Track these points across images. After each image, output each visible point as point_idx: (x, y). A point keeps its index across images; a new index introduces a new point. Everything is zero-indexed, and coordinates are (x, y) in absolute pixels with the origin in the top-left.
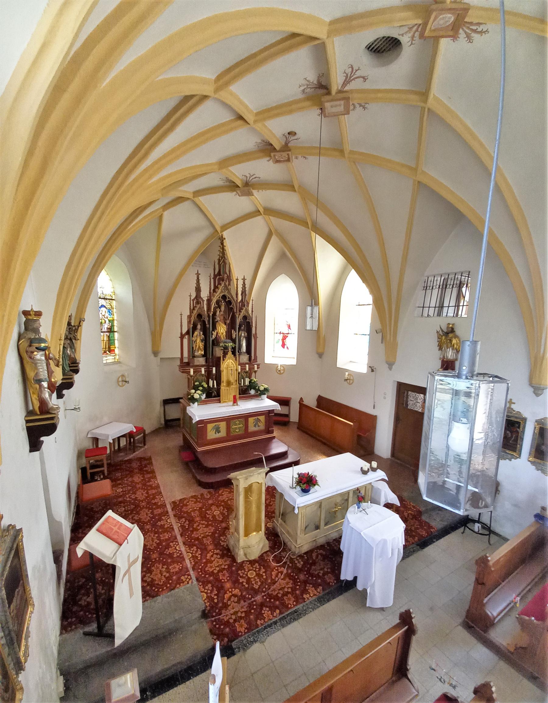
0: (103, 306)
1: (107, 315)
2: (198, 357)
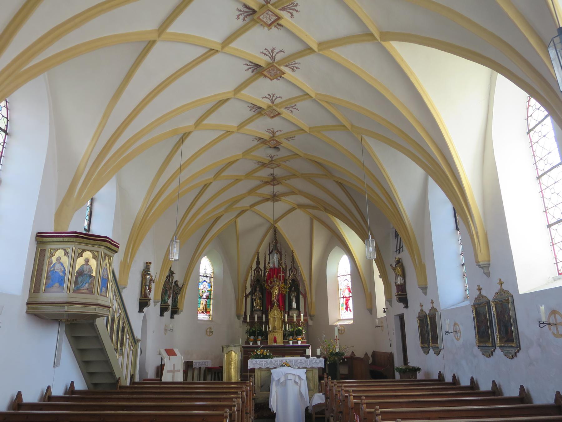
0: (204, 281)
1: (207, 287)
2: (257, 311)
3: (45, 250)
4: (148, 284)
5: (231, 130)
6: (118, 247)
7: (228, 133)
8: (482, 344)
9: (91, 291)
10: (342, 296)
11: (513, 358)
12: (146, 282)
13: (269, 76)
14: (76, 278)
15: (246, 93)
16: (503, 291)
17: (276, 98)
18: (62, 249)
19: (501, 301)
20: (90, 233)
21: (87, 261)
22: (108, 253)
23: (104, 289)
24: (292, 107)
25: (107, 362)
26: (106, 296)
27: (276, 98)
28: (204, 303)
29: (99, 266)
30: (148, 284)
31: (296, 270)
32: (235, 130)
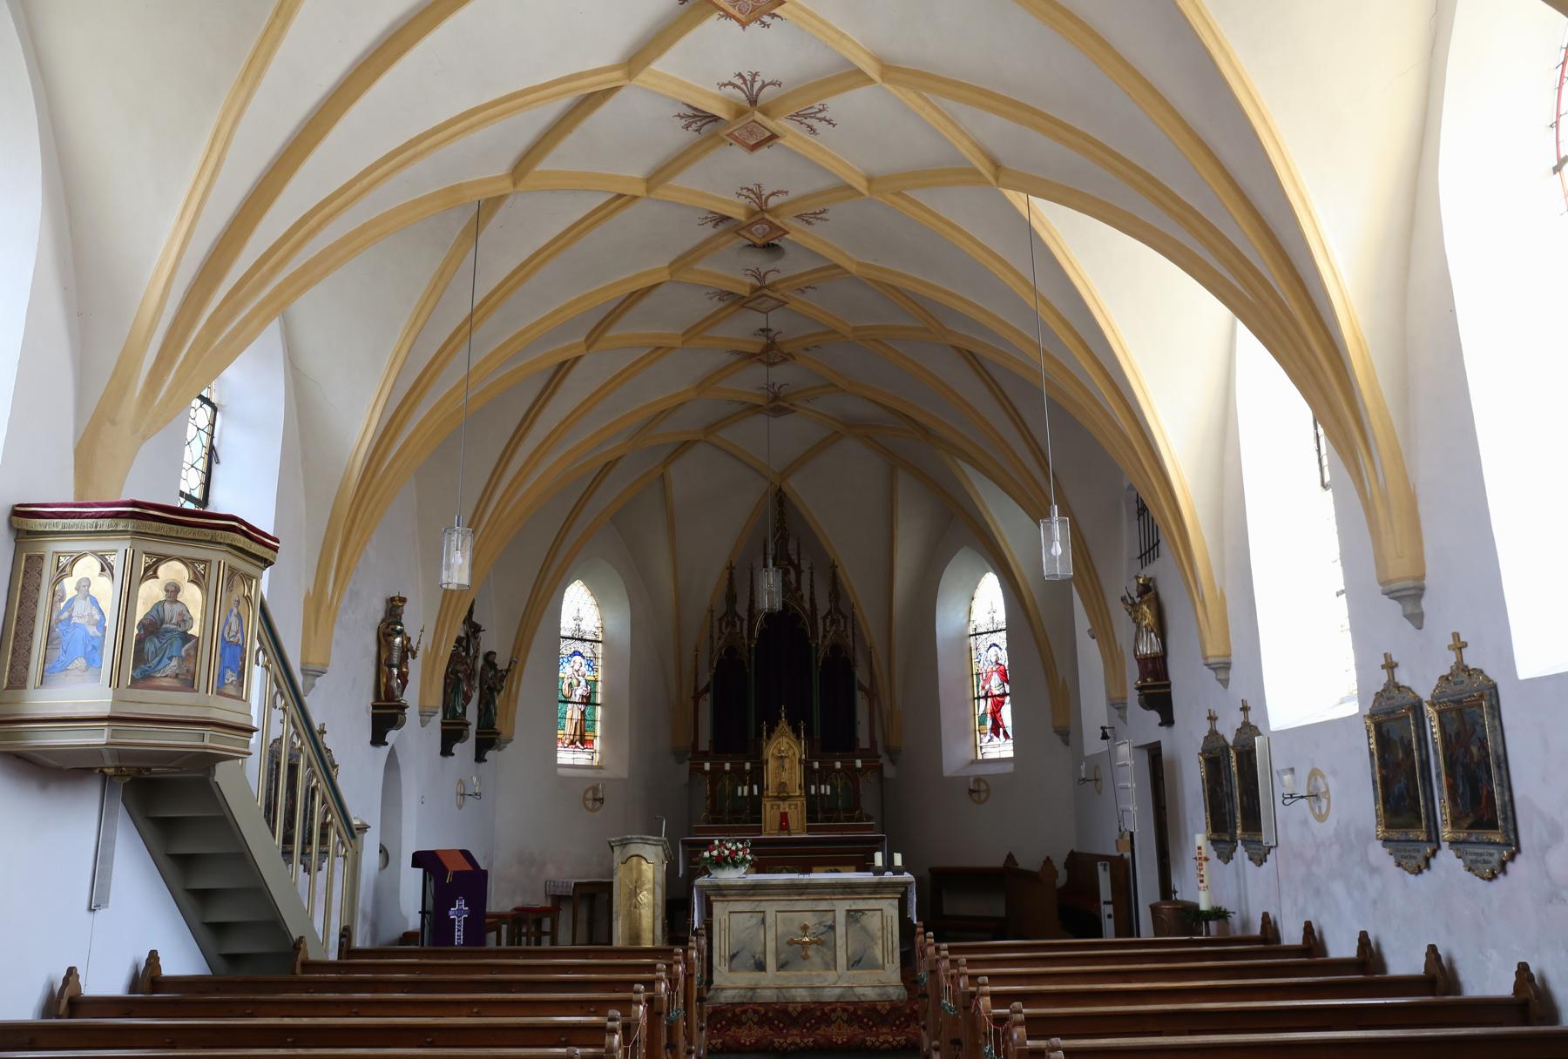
1: (584, 669)
3: (41, 558)
4: (395, 661)
5: (630, 191)
6: (275, 549)
7: (621, 200)
8: (1395, 835)
9: (188, 682)
10: (982, 693)
11: (1493, 877)
12: (390, 657)
13: (735, 12)
14: (140, 641)
15: (665, 65)
16: (1465, 669)
17: (764, 86)
18: (94, 553)
19: (1459, 702)
20: (209, 509)
21: (173, 591)
22: (244, 566)
23: (231, 677)
24: (813, 116)
25: (259, 892)
26: (240, 698)
27: (764, 86)
28: (577, 715)
29: (209, 609)
30: (395, 661)
31: (845, 618)
32: (640, 190)
